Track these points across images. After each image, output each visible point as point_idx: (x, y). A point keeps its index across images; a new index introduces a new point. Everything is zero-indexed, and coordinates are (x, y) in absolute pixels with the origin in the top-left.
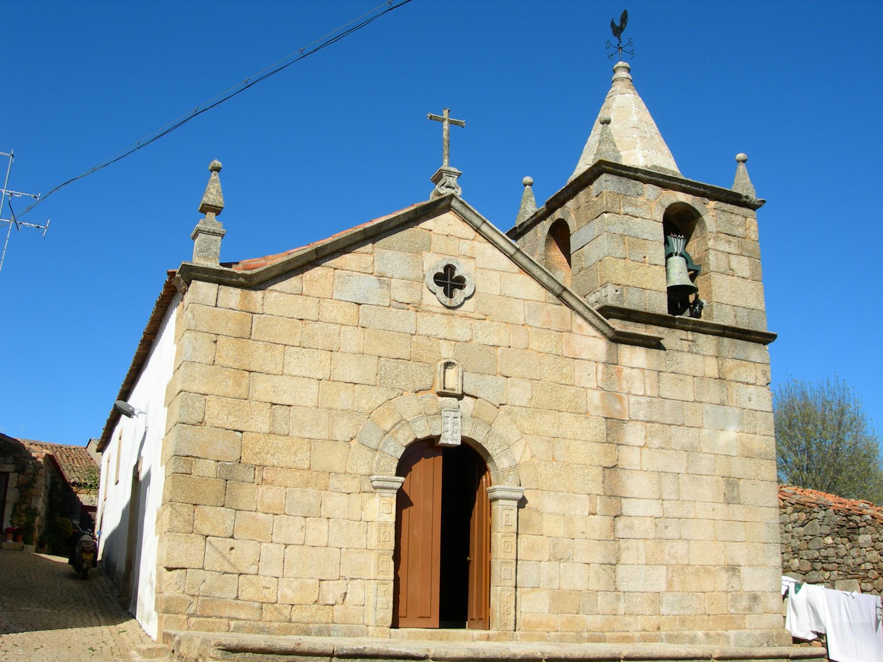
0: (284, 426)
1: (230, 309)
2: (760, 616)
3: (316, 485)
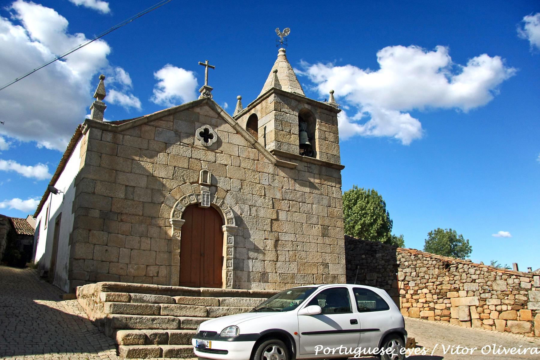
0: (131, 196)
1: (108, 142)
3: (145, 222)
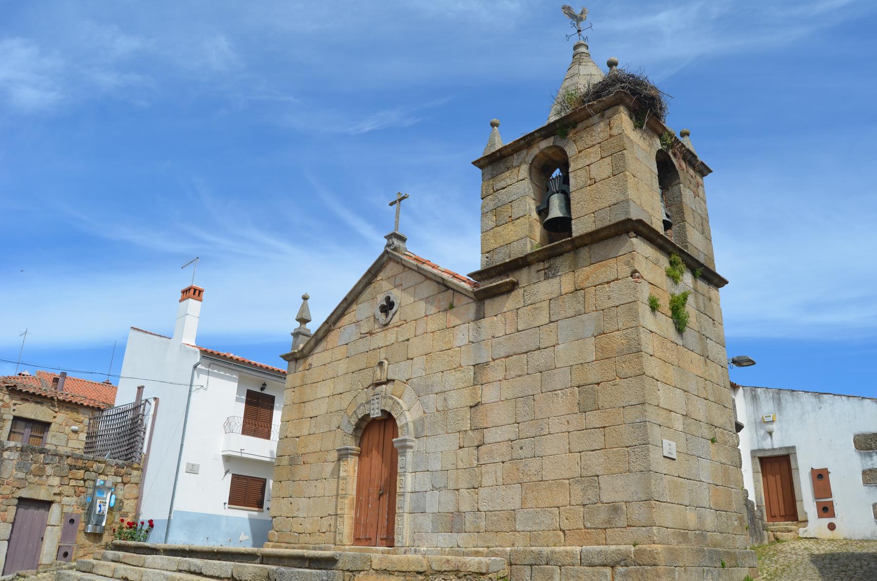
2: (624, 530)
